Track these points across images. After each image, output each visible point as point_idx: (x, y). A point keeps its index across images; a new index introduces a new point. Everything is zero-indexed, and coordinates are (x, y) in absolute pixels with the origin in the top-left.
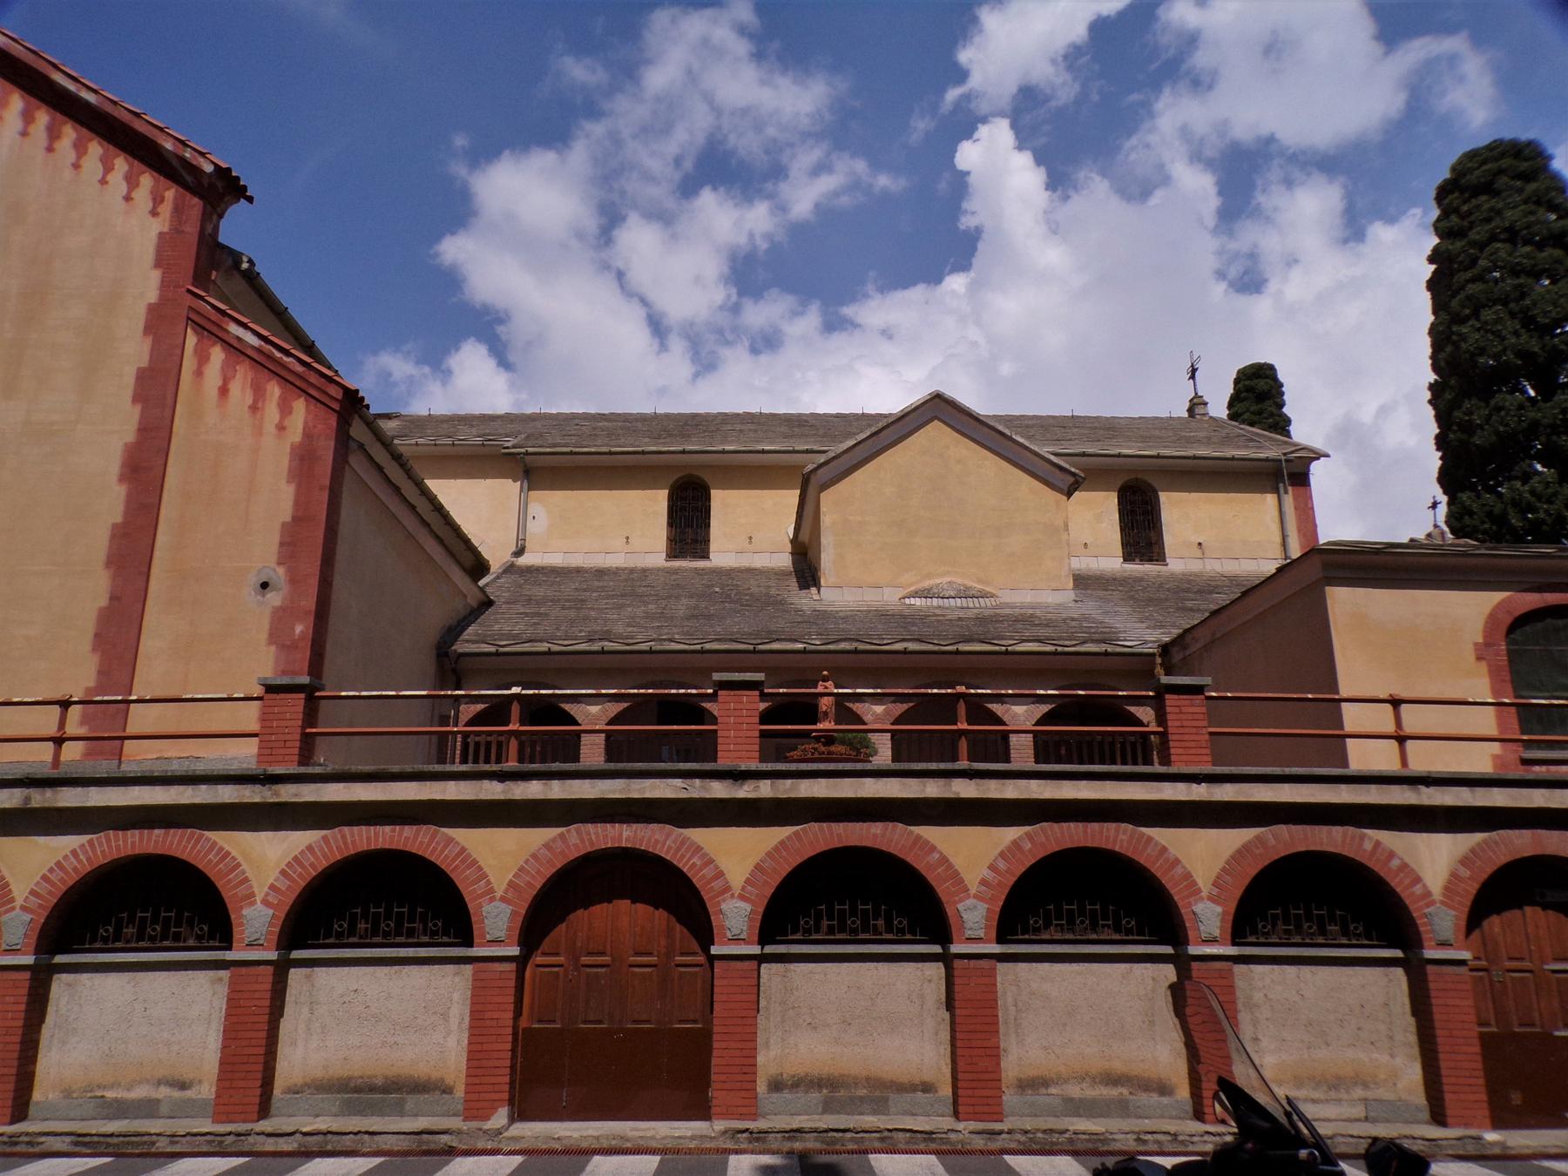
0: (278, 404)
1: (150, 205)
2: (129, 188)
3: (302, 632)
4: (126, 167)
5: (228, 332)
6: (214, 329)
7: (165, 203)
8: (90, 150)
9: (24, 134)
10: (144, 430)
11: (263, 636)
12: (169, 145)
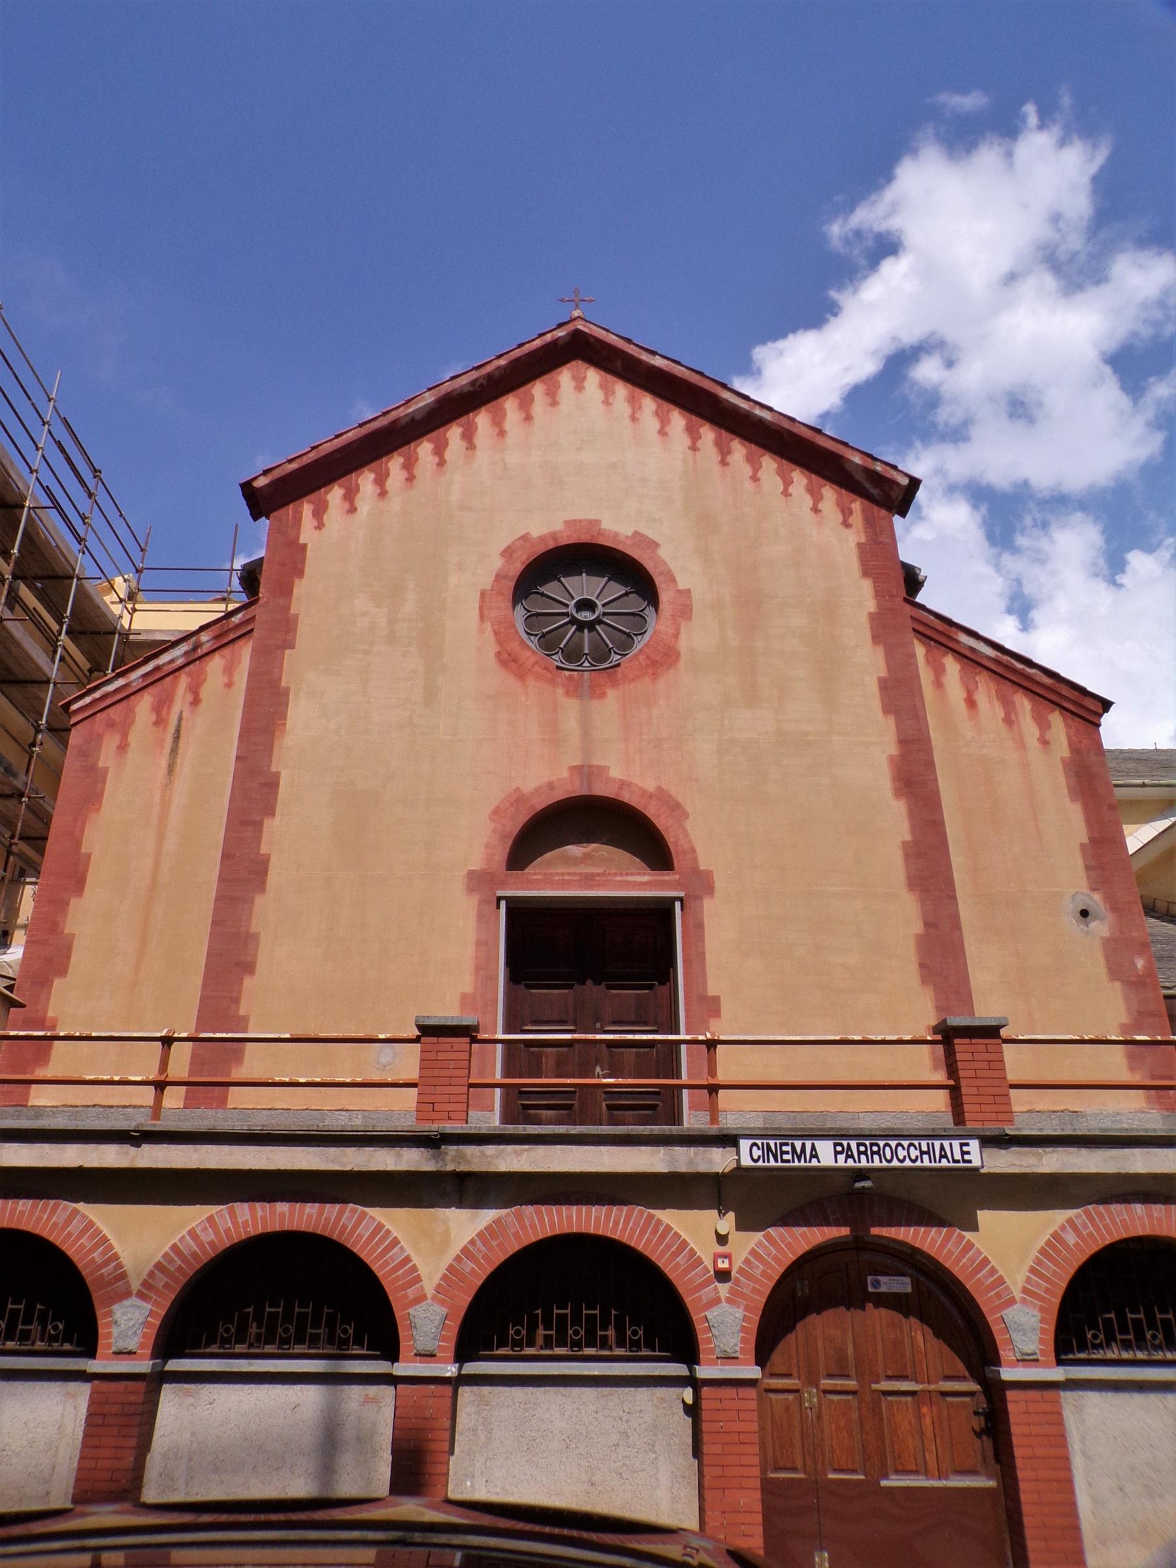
0: (1033, 717)
1: (840, 518)
3: (1143, 966)
4: (805, 481)
5: (958, 642)
6: (943, 640)
7: (854, 514)
8: (764, 464)
9: (694, 448)
10: (904, 742)
11: (1101, 969)
12: (857, 459)
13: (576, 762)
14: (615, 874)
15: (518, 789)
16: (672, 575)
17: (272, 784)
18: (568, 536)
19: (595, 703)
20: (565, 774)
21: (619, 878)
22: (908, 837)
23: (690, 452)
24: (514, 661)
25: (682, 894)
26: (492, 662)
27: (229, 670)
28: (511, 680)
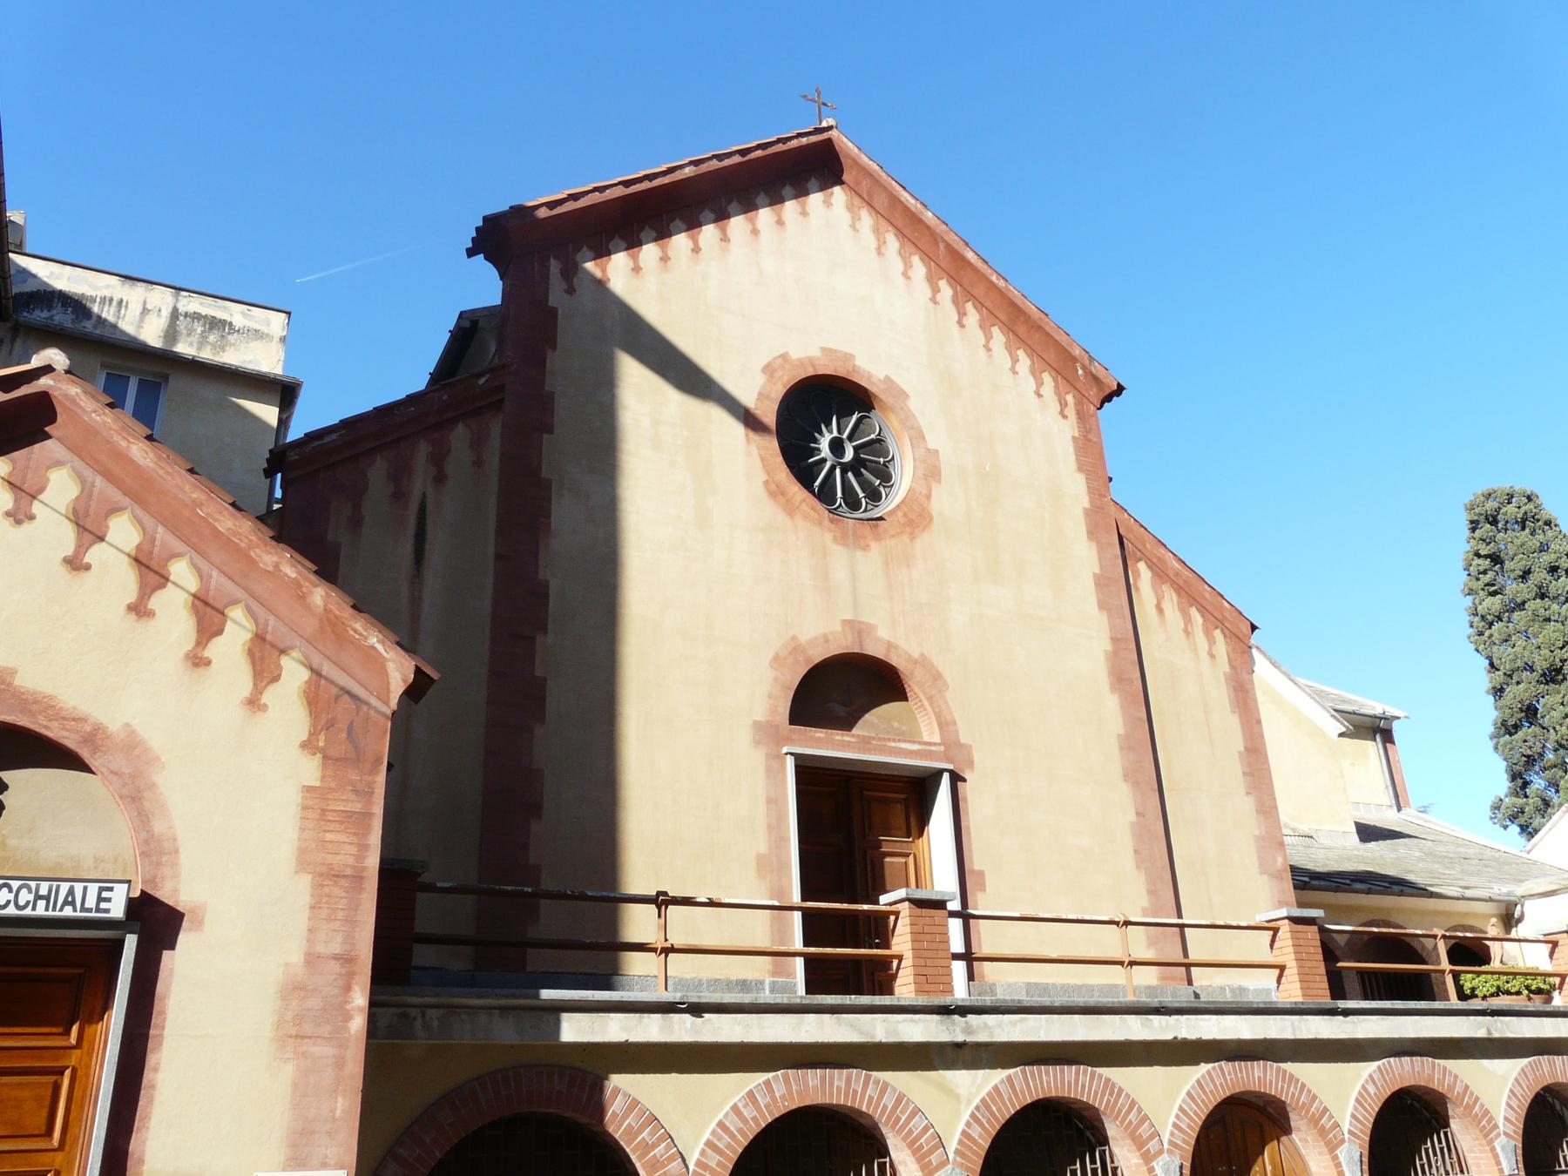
2: (1037, 384)
9: (934, 301)
13: (849, 617)
14: (889, 739)
15: (794, 638)
16: (921, 432)
17: (540, 595)
18: (825, 365)
19: (859, 555)
20: (838, 628)
21: (893, 744)
22: (1122, 731)
23: (931, 305)
24: (783, 494)
25: (951, 767)
26: (761, 492)
27: (478, 443)
28: (781, 517)
